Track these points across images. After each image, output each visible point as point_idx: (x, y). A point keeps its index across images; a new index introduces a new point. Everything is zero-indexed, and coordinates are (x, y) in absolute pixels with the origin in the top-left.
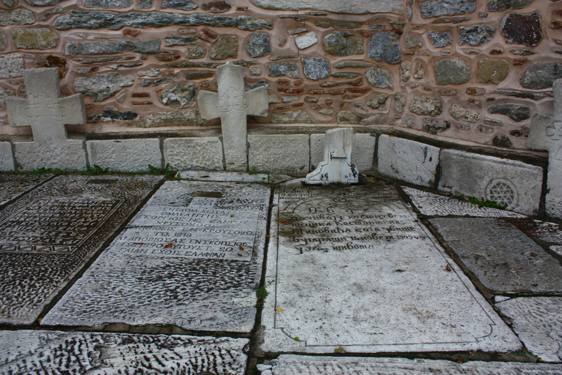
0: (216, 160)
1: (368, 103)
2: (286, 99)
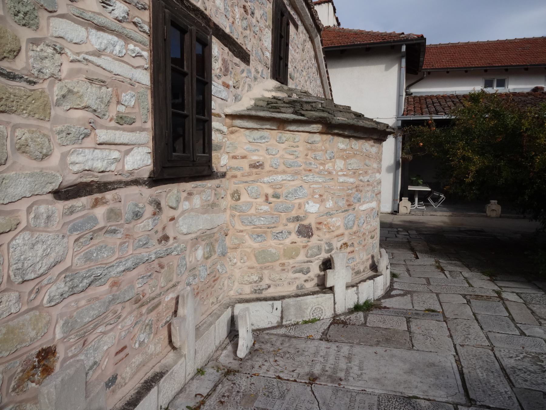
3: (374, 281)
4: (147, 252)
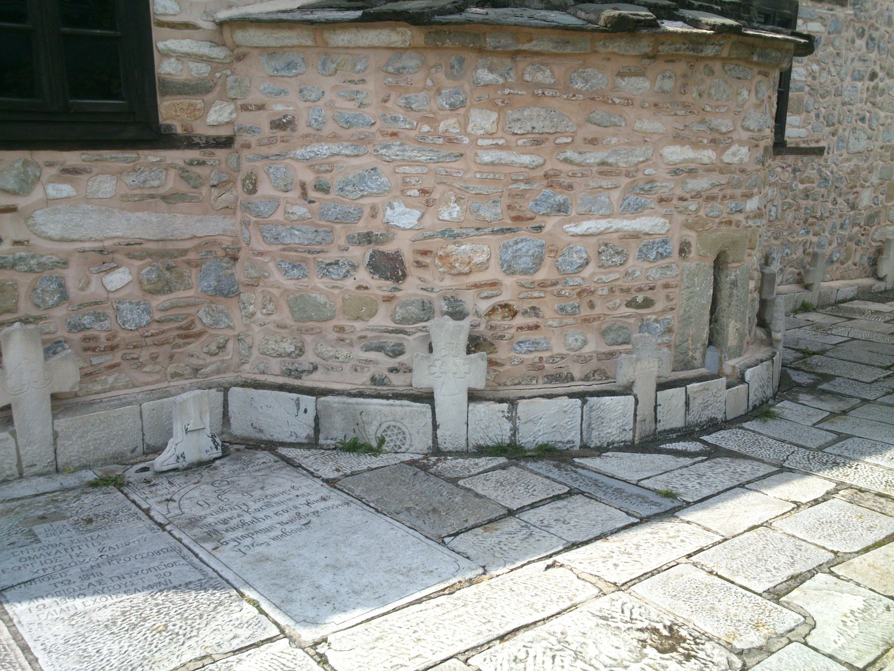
1: (205, 350)
2: (95, 361)
3: (584, 402)
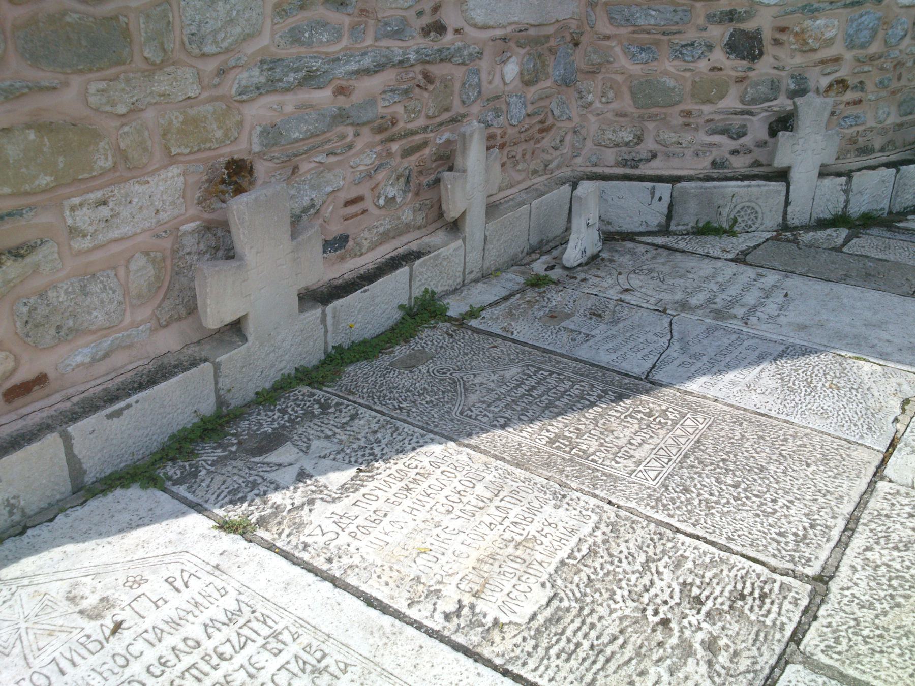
0: (458, 274)
3: (898, 171)
4: (400, 48)
